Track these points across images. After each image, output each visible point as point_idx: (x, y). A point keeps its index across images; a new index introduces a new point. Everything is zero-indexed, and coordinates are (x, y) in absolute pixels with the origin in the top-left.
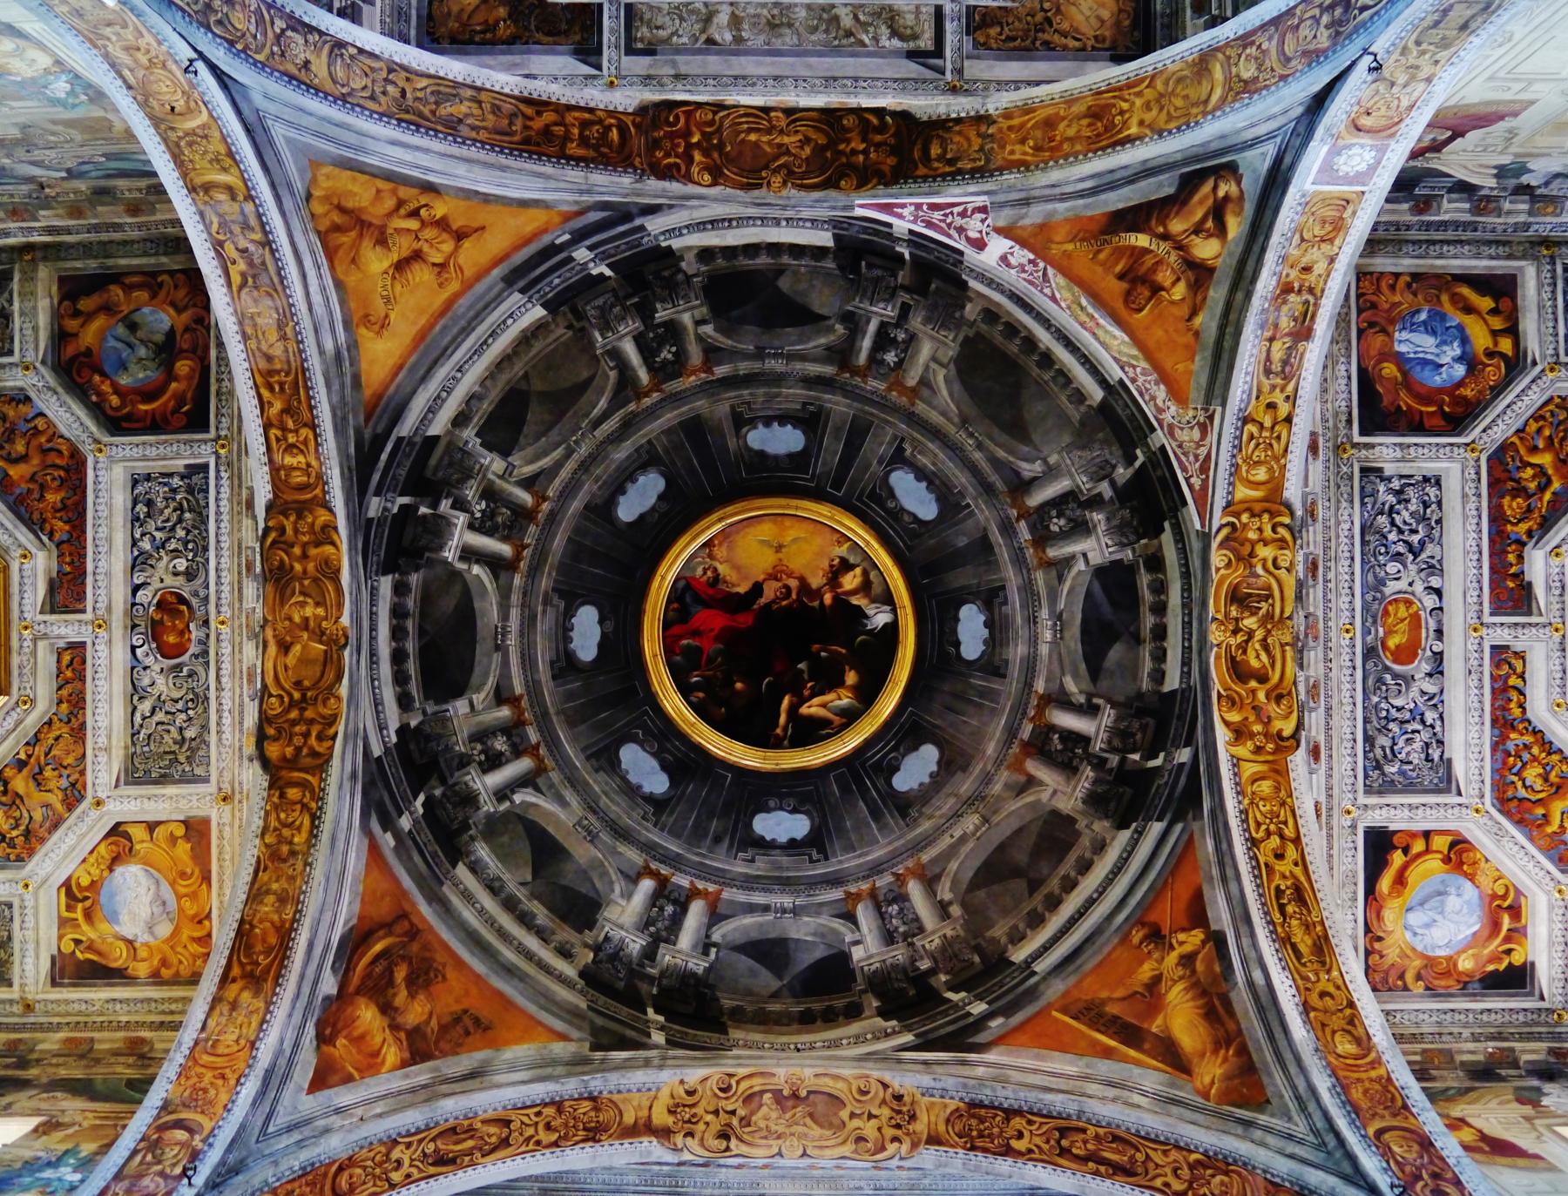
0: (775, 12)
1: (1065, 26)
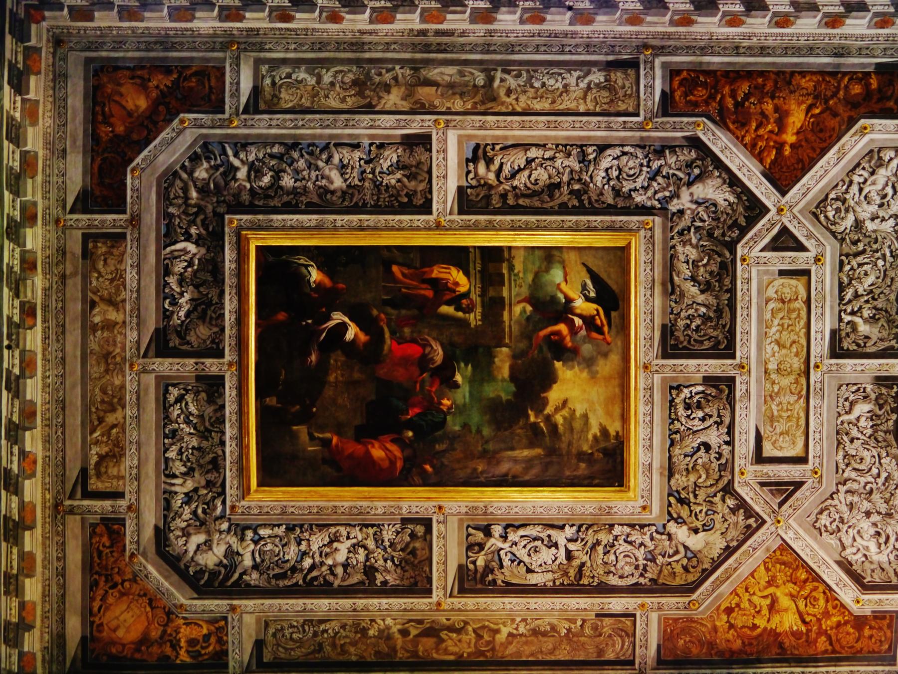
0: (118, 359)
1: (111, 600)
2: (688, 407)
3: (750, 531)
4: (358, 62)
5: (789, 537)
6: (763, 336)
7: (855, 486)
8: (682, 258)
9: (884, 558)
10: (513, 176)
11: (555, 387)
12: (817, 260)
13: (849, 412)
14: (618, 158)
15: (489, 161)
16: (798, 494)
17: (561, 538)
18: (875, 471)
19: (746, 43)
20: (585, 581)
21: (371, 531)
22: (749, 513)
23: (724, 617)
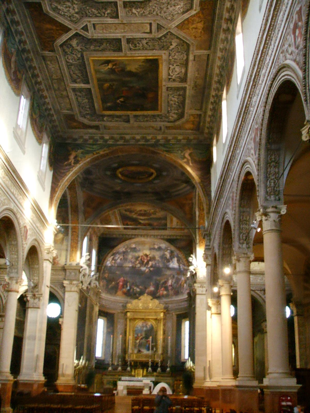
2: (136, 47)
3: (172, 34)
4: (57, 98)
5: (174, 26)
6: (113, 33)
7: (159, 12)
8: (94, 48)
9: (182, 4)
10: (79, 76)
11: (132, 71)
12: (90, 22)
13: (136, 14)
14: (69, 60)
15: (76, 80)
16: (161, 24)
17: (172, 67)
18: (154, 7)
19: (30, 36)
20: (185, 63)
21: (169, 95)
22: (167, 34)
23: (197, 38)
